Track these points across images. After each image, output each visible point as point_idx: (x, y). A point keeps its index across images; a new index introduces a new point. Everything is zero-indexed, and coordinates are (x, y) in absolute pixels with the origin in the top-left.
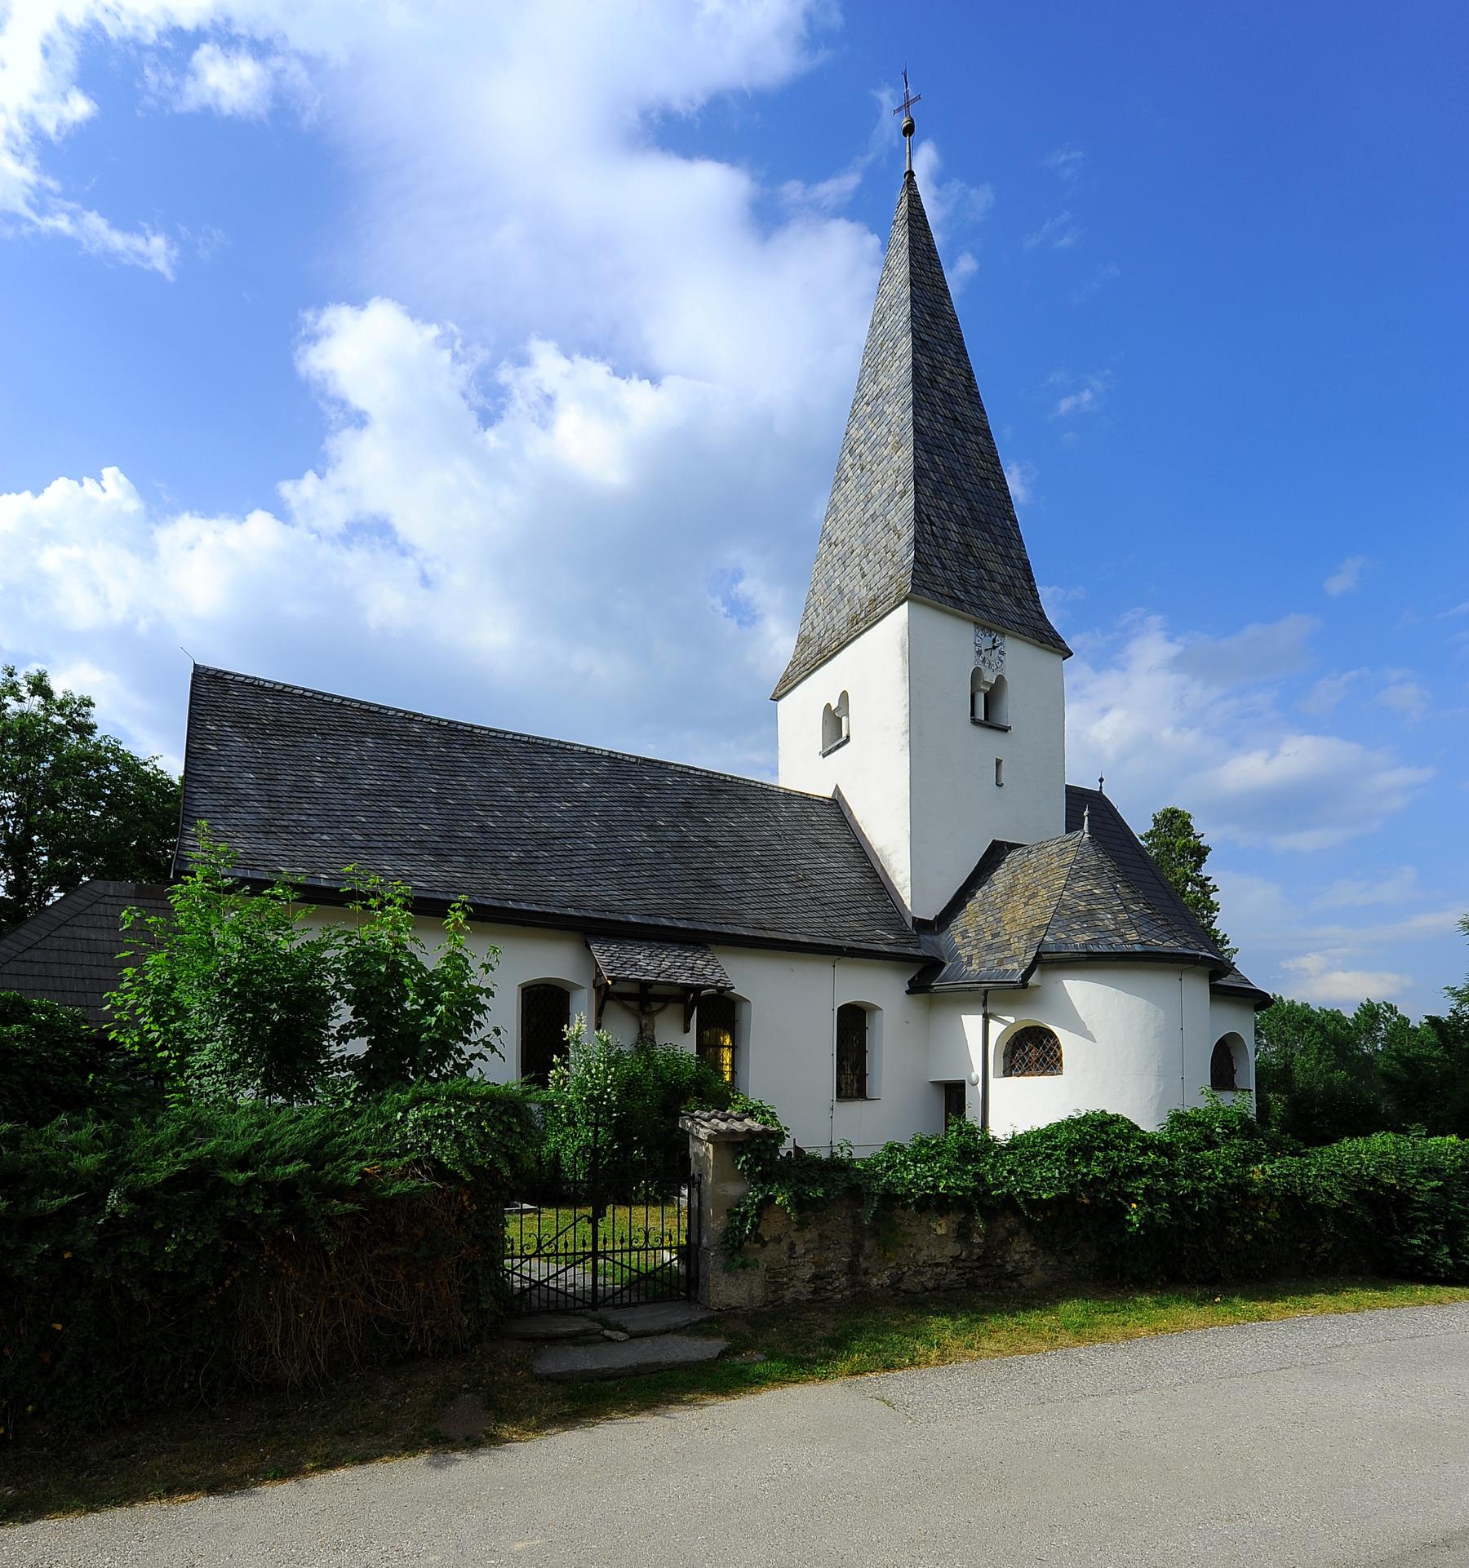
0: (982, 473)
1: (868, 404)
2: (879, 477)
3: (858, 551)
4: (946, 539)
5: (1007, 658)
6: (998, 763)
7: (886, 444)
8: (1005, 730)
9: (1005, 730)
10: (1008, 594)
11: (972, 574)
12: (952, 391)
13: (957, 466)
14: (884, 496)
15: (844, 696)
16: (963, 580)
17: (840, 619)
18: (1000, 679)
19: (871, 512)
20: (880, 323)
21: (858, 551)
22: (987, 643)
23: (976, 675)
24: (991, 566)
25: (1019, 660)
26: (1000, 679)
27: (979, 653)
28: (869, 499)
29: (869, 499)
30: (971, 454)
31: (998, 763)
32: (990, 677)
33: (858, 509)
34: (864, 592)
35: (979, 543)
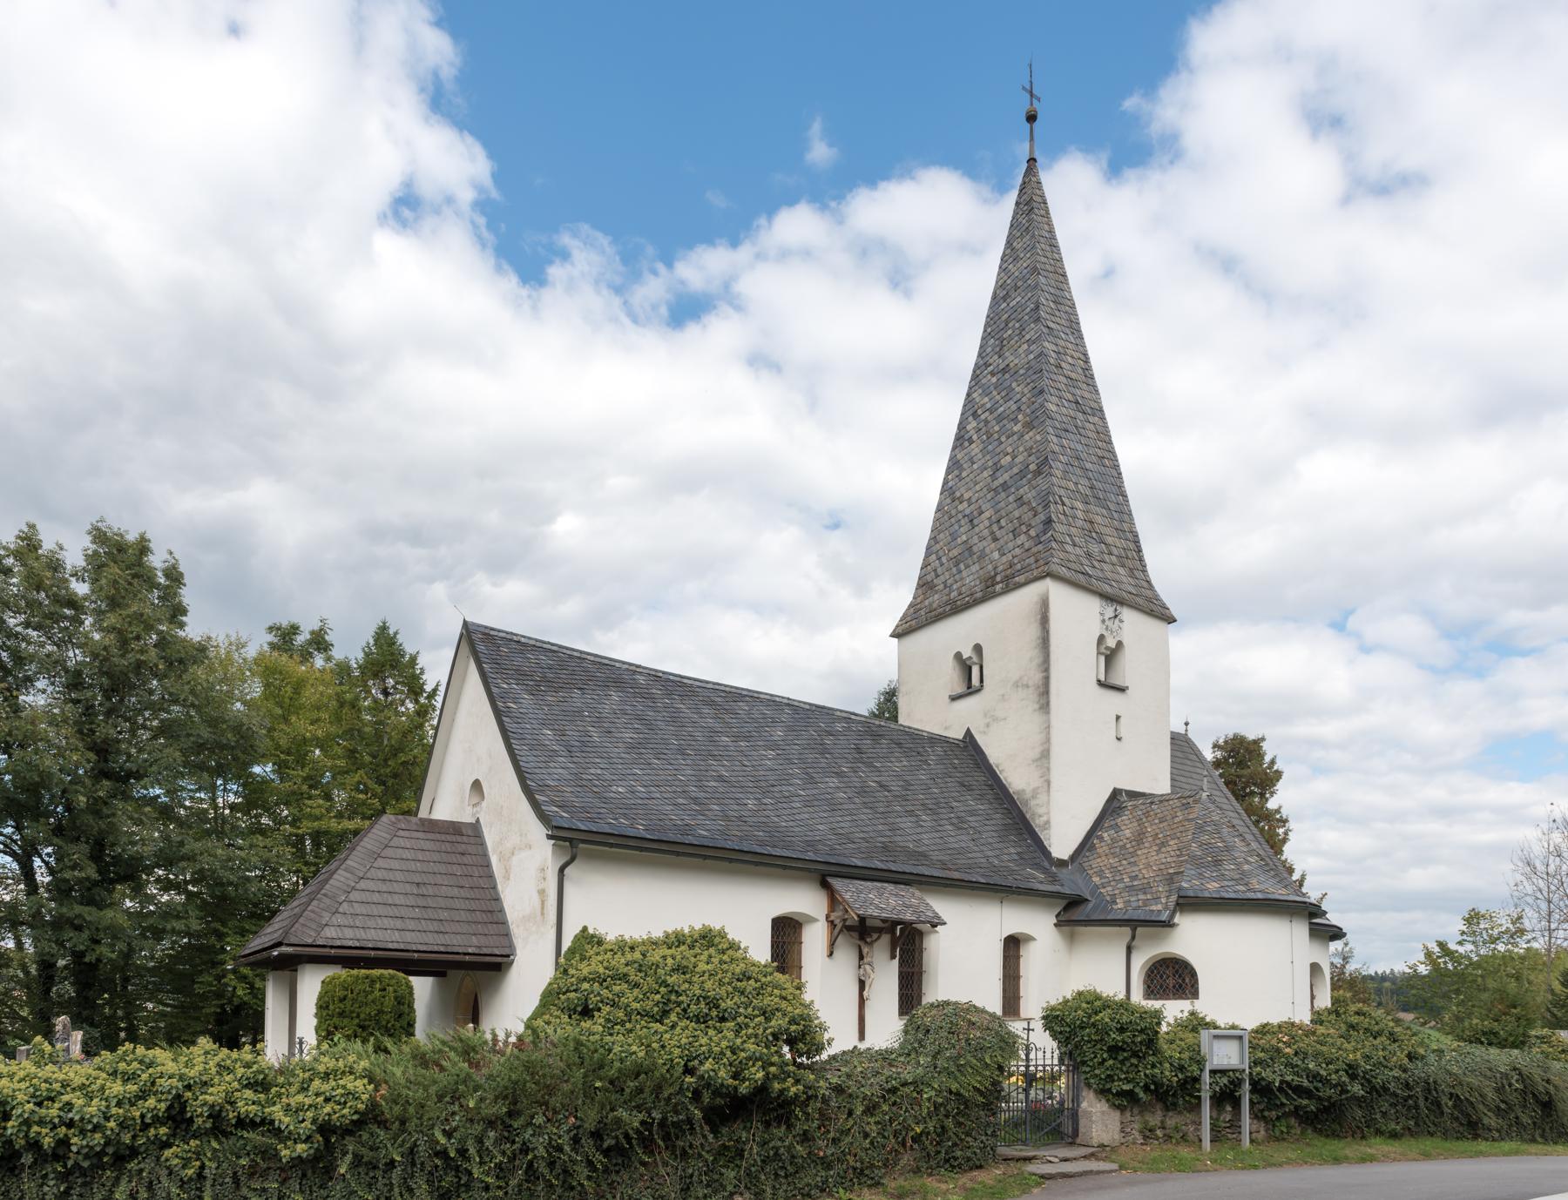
0: (1100, 453)
1: (993, 374)
2: (1009, 450)
3: (987, 514)
4: (1074, 517)
5: (1125, 626)
6: (1118, 718)
7: (1016, 421)
8: (1122, 690)
9: (1122, 690)
10: (1123, 566)
11: (1095, 548)
12: (1073, 375)
13: (1079, 447)
14: (1015, 470)
15: (978, 649)
16: (1089, 555)
17: (971, 577)
18: (1120, 644)
19: (1001, 481)
20: (1004, 299)
21: (987, 514)
22: (1110, 612)
23: (1101, 638)
24: (1109, 540)
25: (1133, 625)
26: (1120, 644)
28: (997, 468)
29: (997, 468)
30: (1090, 434)
31: (1118, 718)
32: (1111, 643)
33: (985, 474)
34: (996, 555)
35: (1099, 519)
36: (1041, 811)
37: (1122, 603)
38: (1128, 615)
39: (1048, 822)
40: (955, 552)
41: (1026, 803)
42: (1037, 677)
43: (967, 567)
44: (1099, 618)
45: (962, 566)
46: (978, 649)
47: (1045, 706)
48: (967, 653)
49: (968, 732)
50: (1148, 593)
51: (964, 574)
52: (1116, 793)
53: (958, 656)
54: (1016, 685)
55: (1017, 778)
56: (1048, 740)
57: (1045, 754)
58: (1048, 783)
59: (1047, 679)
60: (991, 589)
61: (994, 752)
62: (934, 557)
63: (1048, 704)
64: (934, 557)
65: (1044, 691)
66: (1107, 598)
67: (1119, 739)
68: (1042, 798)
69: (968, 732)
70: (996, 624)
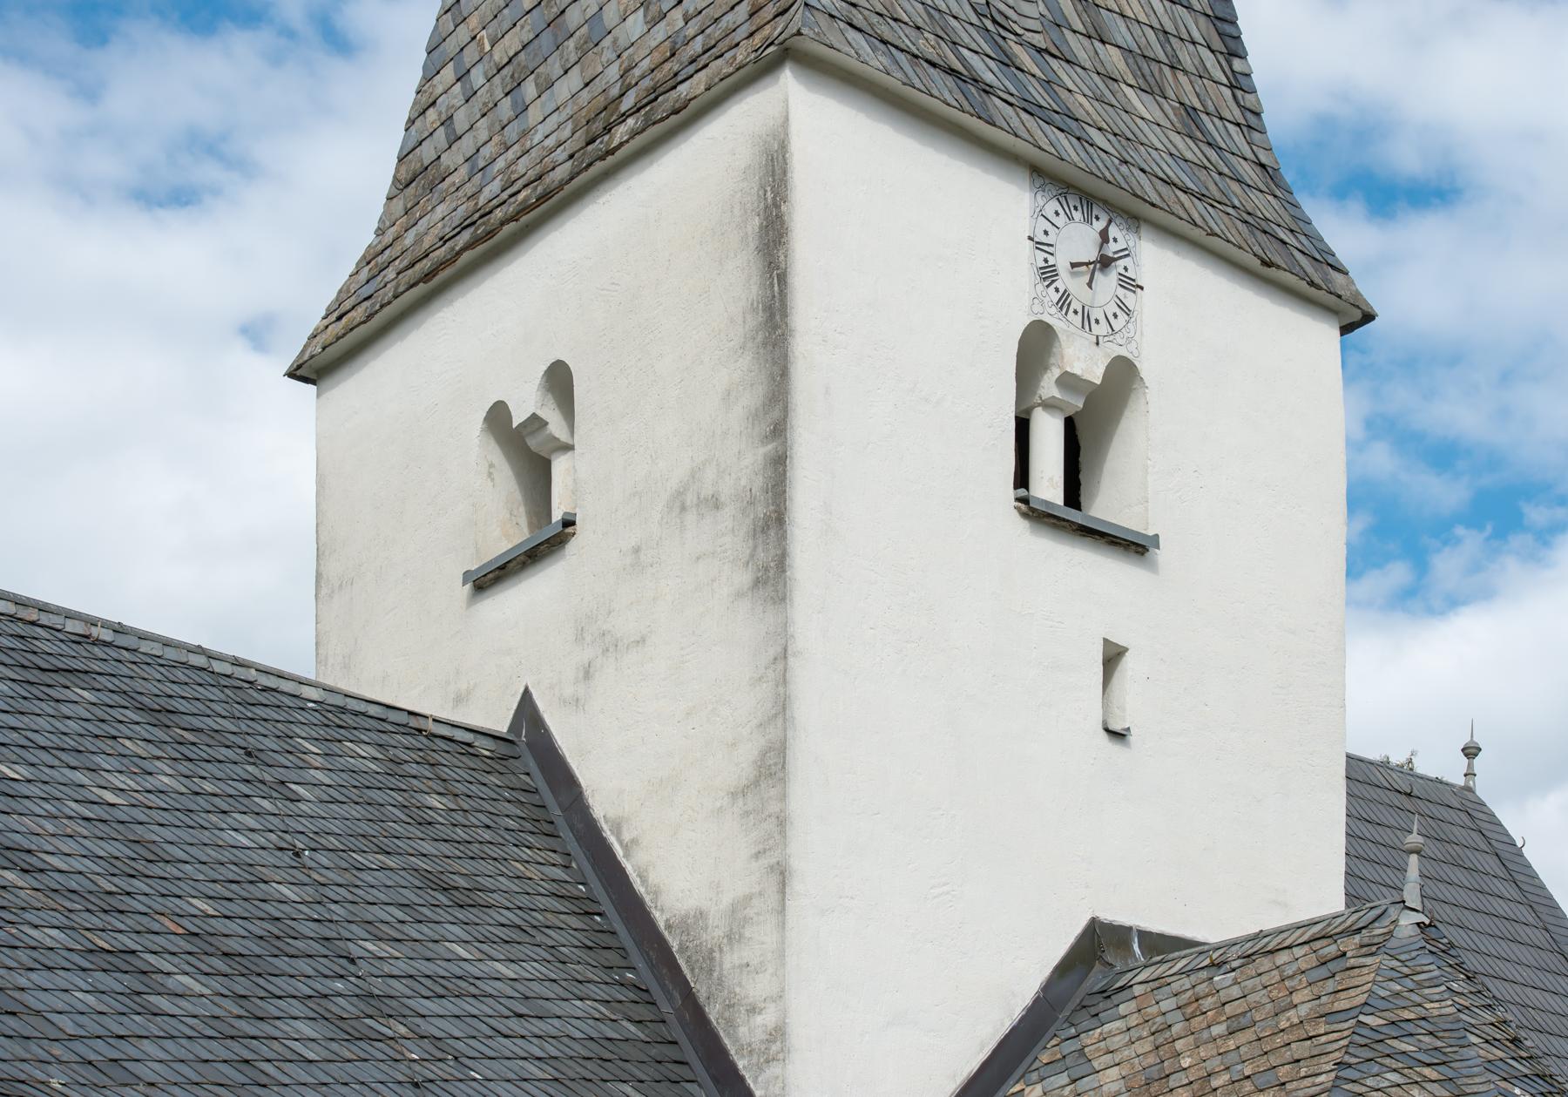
5: (1142, 303)
6: (1113, 657)
8: (1134, 547)
10: (1152, 89)
15: (559, 380)
17: (550, 120)
22: (1077, 238)
27: (1048, 274)
31: (1113, 657)
32: (1083, 358)
36: (756, 988)
37: (1134, 220)
38: (1152, 259)
39: (778, 1033)
40: (511, 43)
41: (709, 960)
42: (744, 463)
43: (547, 86)
44: (1026, 260)
45: (529, 89)
46: (559, 380)
47: (771, 577)
48: (526, 401)
49: (527, 709)
50: (1264, 205)
51: (534, 114)
52: (1099, 945)
53: (497, 416)
54: (679, 504)
55: (679, 866)
56: (781, 709)
57: (773, 767)
58: (782, 875)
59: (779, 466)
60: (606, 148)
61: (612, 775)
62: (448, 74)
63: (781, 562)
64: (448, 74)
65: (772, 517)
66: (1044, 175)
67: (1118, 736)
68: (762, 935)
69: (527, 709)
70: (623, 272)
